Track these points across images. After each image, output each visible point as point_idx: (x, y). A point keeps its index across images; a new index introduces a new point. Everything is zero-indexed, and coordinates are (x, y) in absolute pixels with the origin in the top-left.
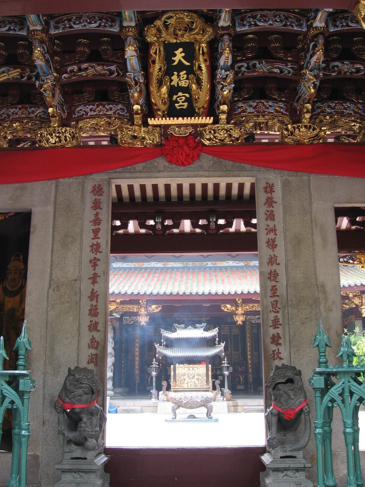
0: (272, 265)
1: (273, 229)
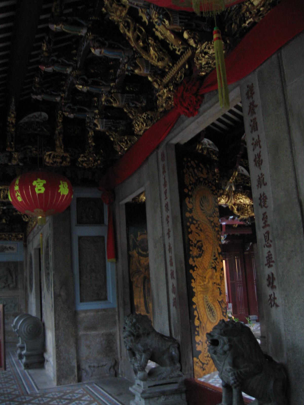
0: (261, 187)
1: (258, 140)
